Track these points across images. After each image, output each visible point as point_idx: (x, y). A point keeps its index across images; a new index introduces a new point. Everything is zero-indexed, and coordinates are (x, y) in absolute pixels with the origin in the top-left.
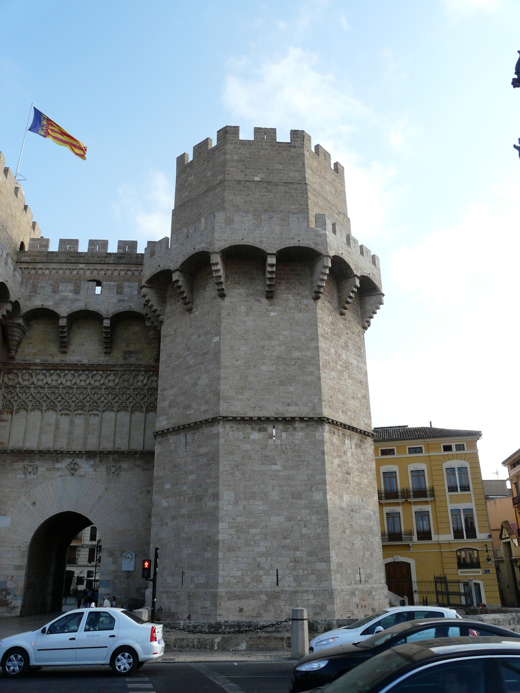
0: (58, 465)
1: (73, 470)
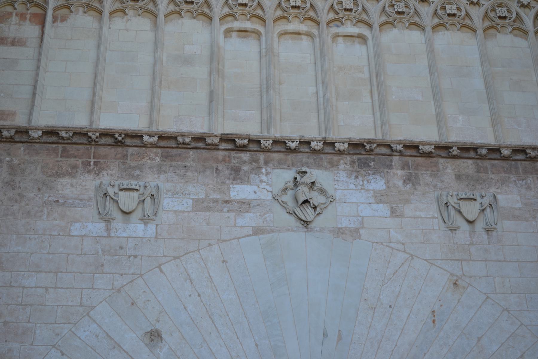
0: (240, 191)
1: (305, 208)
